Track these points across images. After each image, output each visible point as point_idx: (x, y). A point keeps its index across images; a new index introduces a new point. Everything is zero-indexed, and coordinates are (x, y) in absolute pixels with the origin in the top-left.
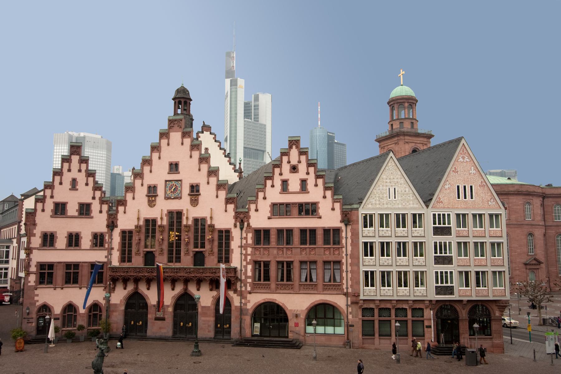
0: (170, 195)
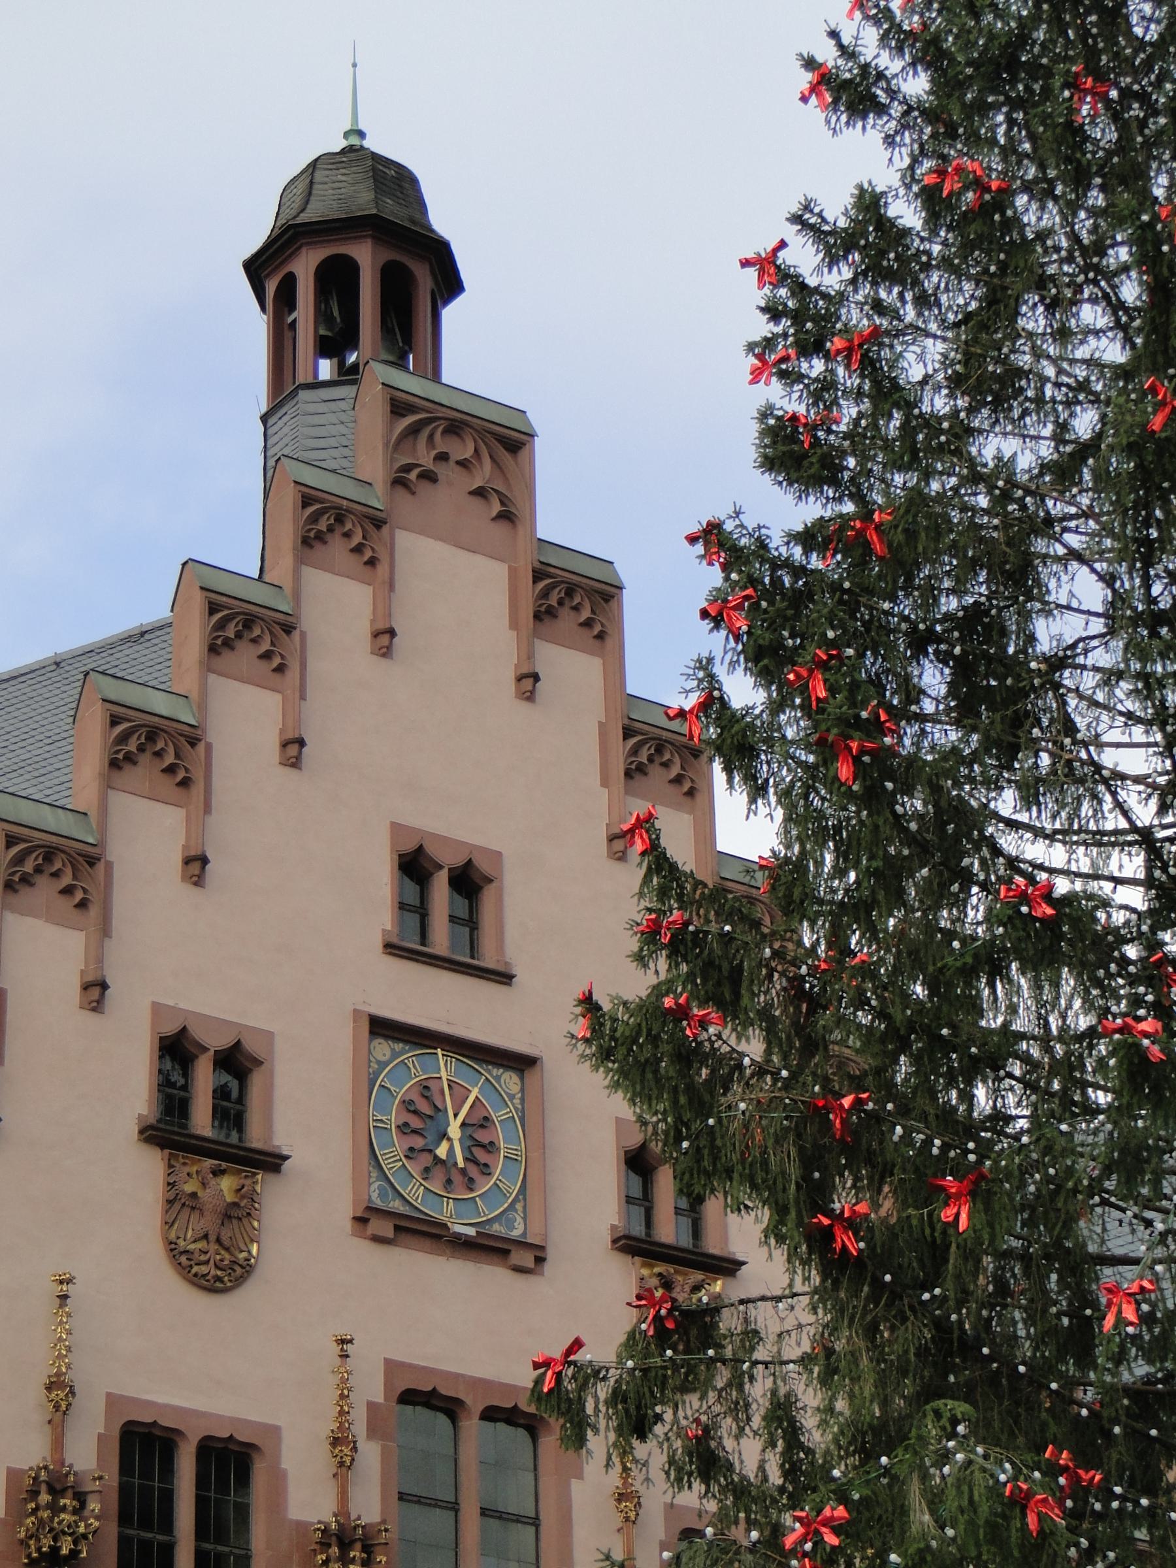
0: (418, 1194)
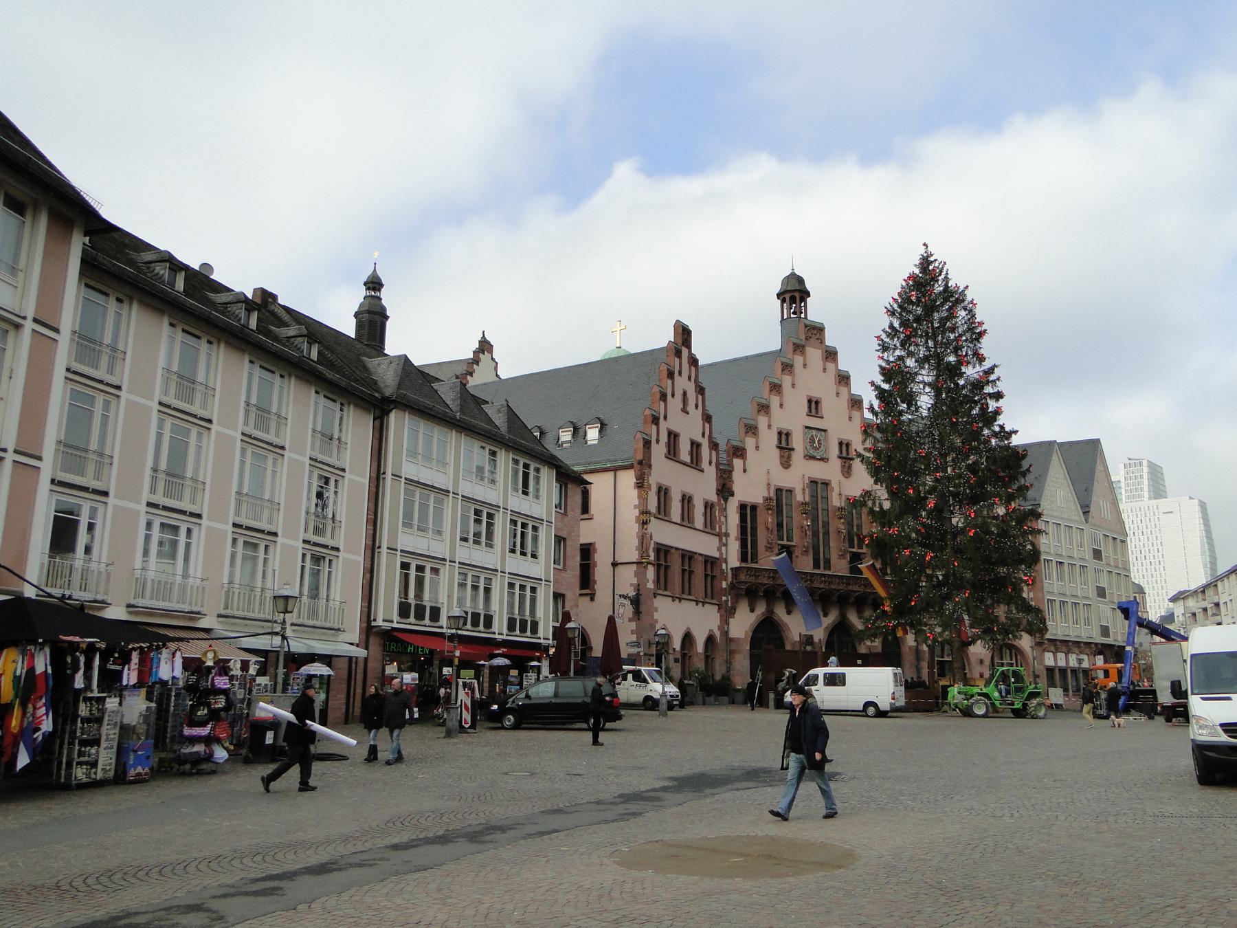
0: (811, 452)
